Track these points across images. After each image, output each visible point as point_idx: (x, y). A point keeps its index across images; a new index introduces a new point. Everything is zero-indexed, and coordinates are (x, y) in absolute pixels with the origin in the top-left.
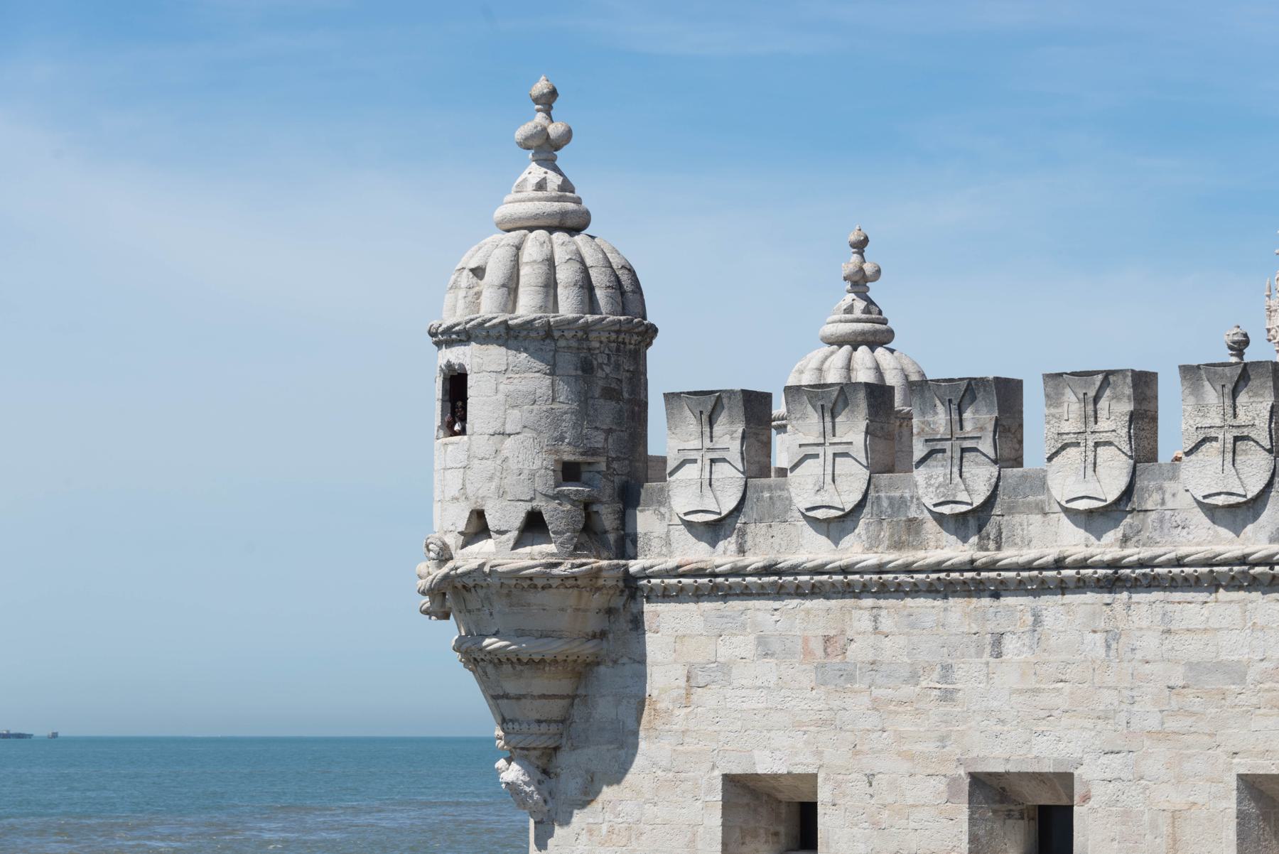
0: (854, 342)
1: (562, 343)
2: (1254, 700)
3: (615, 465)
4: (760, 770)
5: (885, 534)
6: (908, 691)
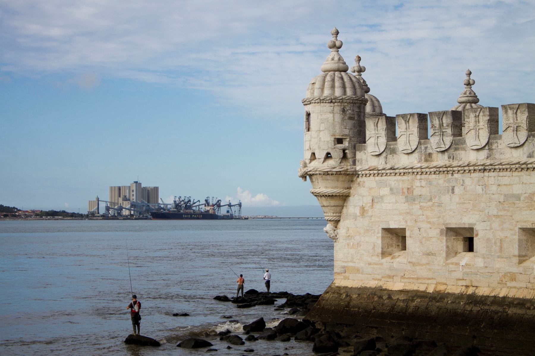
0: (471, 102)
1: (336, 104)
2: (523, 206)
3: (353, 139)
4: (391, 227)
5: (423, 158)
6: (430, 203)
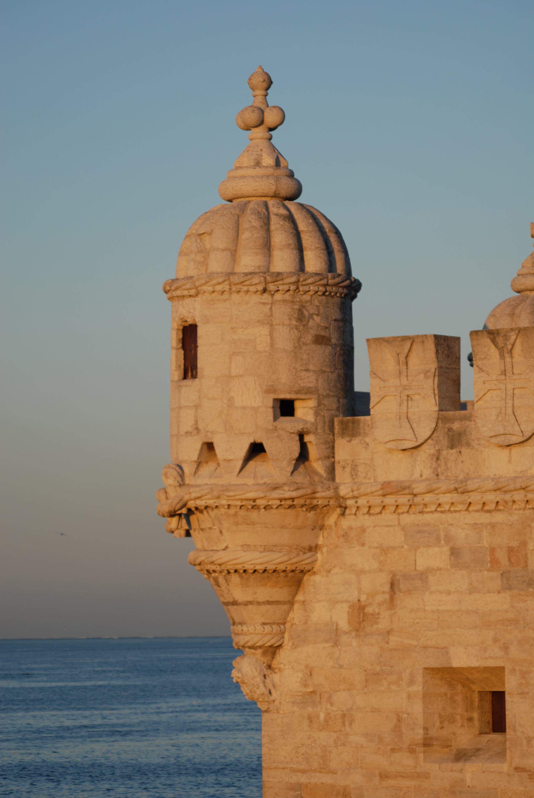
3: (326, 402)
4: (456, 664)
